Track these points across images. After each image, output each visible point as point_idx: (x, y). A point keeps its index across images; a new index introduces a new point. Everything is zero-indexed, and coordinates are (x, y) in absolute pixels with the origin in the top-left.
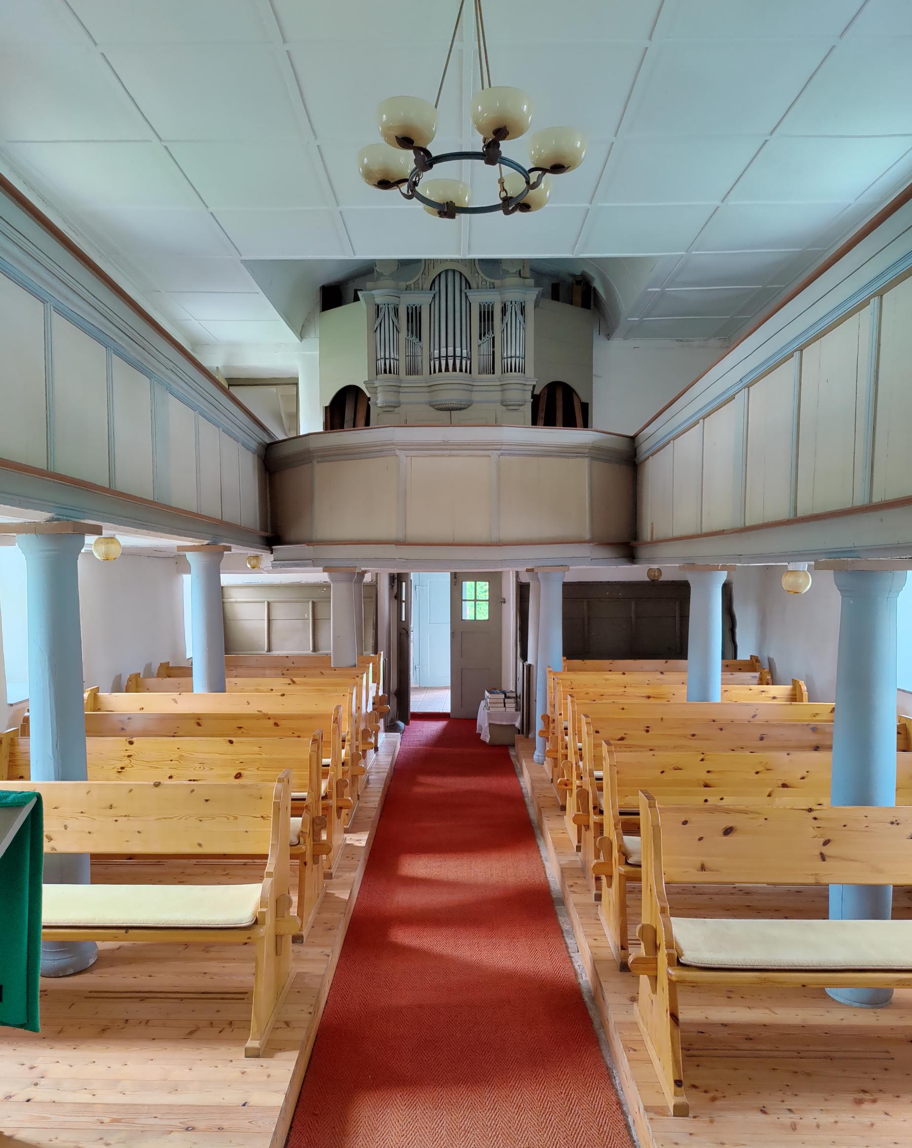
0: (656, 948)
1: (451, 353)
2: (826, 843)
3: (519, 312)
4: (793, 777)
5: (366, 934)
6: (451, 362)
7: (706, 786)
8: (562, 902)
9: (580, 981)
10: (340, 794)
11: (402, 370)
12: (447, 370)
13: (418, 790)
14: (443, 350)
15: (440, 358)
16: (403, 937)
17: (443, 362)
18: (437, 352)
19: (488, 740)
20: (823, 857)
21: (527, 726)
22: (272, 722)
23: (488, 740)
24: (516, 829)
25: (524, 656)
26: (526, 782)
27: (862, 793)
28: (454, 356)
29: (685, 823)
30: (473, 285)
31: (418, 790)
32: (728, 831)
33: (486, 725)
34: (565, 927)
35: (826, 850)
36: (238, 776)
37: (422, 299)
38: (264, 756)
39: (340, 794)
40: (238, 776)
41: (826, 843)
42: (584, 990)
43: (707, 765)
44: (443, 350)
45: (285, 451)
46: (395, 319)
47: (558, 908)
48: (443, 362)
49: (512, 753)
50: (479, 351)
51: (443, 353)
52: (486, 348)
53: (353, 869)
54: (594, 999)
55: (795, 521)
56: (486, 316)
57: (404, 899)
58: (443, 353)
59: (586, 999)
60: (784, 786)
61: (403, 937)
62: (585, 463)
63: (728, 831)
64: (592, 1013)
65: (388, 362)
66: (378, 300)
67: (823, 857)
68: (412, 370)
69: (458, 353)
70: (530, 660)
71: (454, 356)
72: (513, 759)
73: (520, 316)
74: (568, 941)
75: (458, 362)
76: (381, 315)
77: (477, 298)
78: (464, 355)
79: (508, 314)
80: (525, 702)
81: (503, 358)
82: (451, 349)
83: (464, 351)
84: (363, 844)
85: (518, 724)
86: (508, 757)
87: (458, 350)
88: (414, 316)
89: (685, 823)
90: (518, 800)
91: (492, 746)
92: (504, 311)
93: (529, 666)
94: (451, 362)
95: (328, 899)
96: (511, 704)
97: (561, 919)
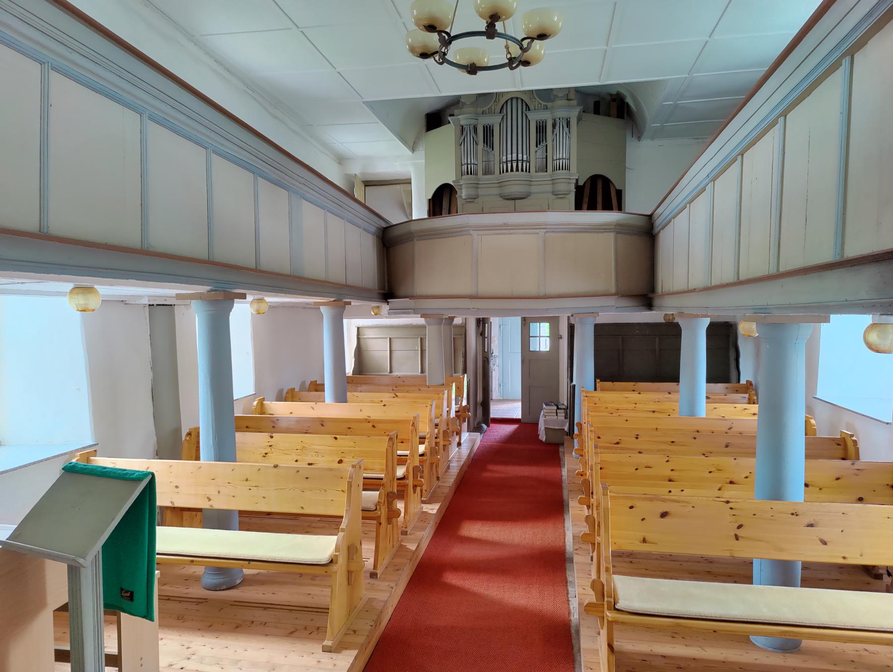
1: (514, 158)
2: (740, 527)
3: (565, 126)
4: (738, 476)
5: (426, 575)
6: (515, 165)
7: (670, 480)
8: (571, 561)
9: (572, 618)
11: (480, 172)
12: (512, 170)
13: (486, 475)
15: (507, 162)
16: (452, 578)
17: (509, 165)
18: (504, 157)
19: (544, 440)
20: (737, 537)
22: (371, 424)
23: (544, 440)
24: (552, 506)
25: (572, 381)
26: (564, 472)
27: (776, 491)
28: (517, 160)
29: (631, 507)
30: (532, 107)
31: (486, 475)
32: (664, 515)
33: (543, 428)
34: (570, 579)
35: (740, 532)
36: (340, 462)
37: (494, 120)
38: (357, 449)
39: (415, 477)
40: (340, 462)
41: (740, 527)
43: (671, 465)
45: (395, 232)
47: (568, 565)
49: (561, 449)
50: (536, 155)
51: (509, 159)
52: (540, 153)
53: (424, 529)
54: (578, 632)
55: (739, 283)
56: (541, 129)
57: (459, 552)
58: (509, 159)
59: (573, 631)
60: (731, 482)
61: (452, 578)
62: (612, 236)
63: (664, 515)
66: (462, 123)
67: (737, 537)
68: (487, 172)
69: (520, 158)
70: (574, 383)
71: (517, 160)
72: (561, 454)
73: (566, 129)
74: (570, 589)
75: (520, 164)
76: (465, 133)
77: (534, 117)
78: (525, 159)
79: (557, 127)
82: (514, 155)
83: (525, 156)
84: (435, 512)
85: (566, 429)
86: (558, 451)
87: (520, 156)
88: (488, 132)
89: (631, 507)
90: (557, 485)
91: (547, 444)
92: (554, 126)
93: (574, 386)
94: (515, 165)
96: (561, 414)
97: (568, 573)
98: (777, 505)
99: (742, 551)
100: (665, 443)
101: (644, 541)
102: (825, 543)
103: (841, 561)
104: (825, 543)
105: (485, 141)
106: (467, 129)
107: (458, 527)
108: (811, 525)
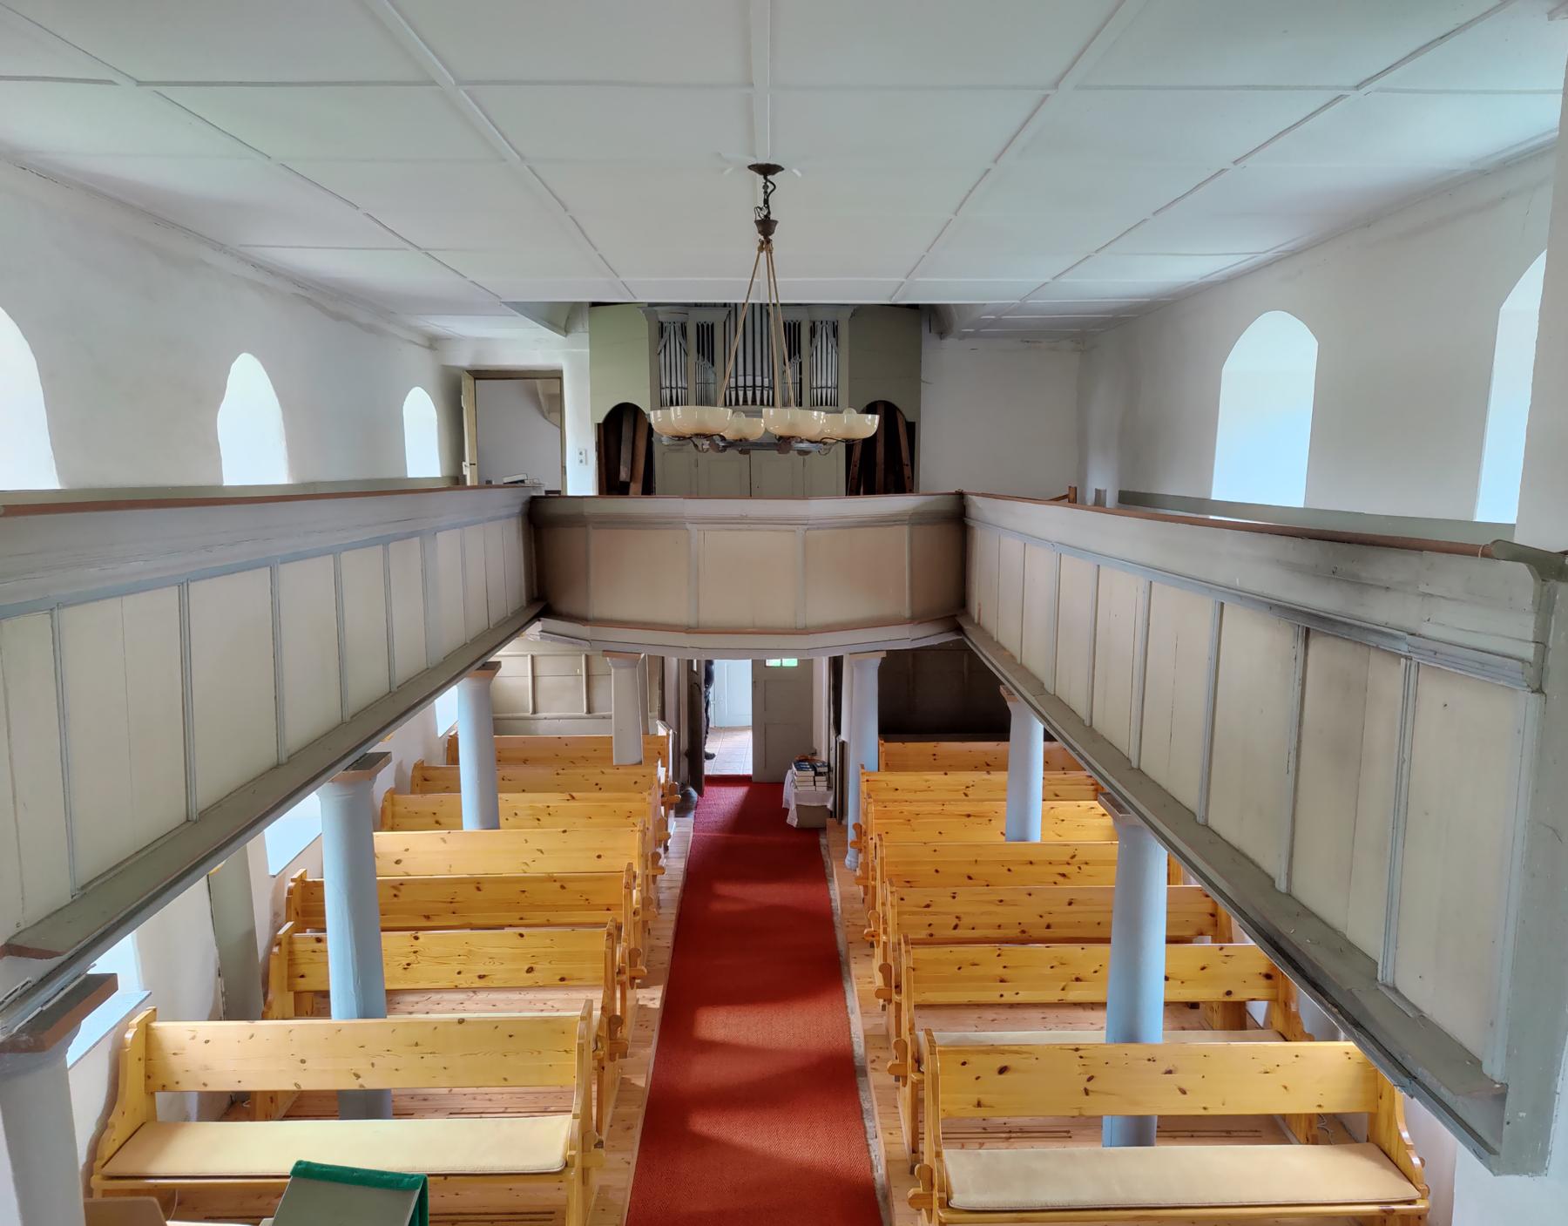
0: (932, 1185)
1: (749, 382)
2: (1090, 1079)
5: (666, 1122)
6: (750, 394)
8: (865, 1073)
9: (876, 1175)
10: (633, 964)
12: (745, 402)
13: (717, 906)
14: (741, 379)
16: (703, 1124)
17: (741, 394)
19: (795, 824)
20: (1087, 1092)
21: (840, 811)
23: (795, 824)
25: (838, 731)
26: (836, 890)
28: (754, 386)
31: (717, 906)
32: (1003, 1070)
33: (793, 807)
34: (866, 1106)
35: (1089, 1086)
39: (633, 964)
41: (1090, 1079)
42: (878, 1186)
43: (1004, 961)
44: (741, 379)
45: (557, 508)
47: (860, 1079)
48: (741, 394)
49: (823, 841)
51: (741, 383)
53: (648, 1044)
54: (886, 1197)
57: (705, 1072)
58: (741, 383)
59: (879, 1198)
60: (1077, 979)
61: (703, 1124)
62: (905, 530)
63: (1003, 1070)
64: (883, 1214)
67: (1087, 1092)
69: (758, 383)
70: (843, 737)
71: (754, 386)
72: (824, 852)
74: (868, 1124)
76: (666, 335)
79: (818, 336)
80: (837, 776)
84: (657, 1004)
85: (829, 806)
86: (817, 846)
87: (758, 379)
91: (800, 830)
93: (843, 744)
94: (750, 394)
95: (625, 1083)
96: (822, 782)
97: (862, 1094)
98: (1131, 1048)
99: (1092, 1106)
100: (991, 902)
101: (979, 1105)
102: (1184, 1092)
103: (1202, 1112)
104: (1184, 1092)
105: (701, 350)
106: (670, 329)
107: (690, 1024)
108: (1170, 1072)
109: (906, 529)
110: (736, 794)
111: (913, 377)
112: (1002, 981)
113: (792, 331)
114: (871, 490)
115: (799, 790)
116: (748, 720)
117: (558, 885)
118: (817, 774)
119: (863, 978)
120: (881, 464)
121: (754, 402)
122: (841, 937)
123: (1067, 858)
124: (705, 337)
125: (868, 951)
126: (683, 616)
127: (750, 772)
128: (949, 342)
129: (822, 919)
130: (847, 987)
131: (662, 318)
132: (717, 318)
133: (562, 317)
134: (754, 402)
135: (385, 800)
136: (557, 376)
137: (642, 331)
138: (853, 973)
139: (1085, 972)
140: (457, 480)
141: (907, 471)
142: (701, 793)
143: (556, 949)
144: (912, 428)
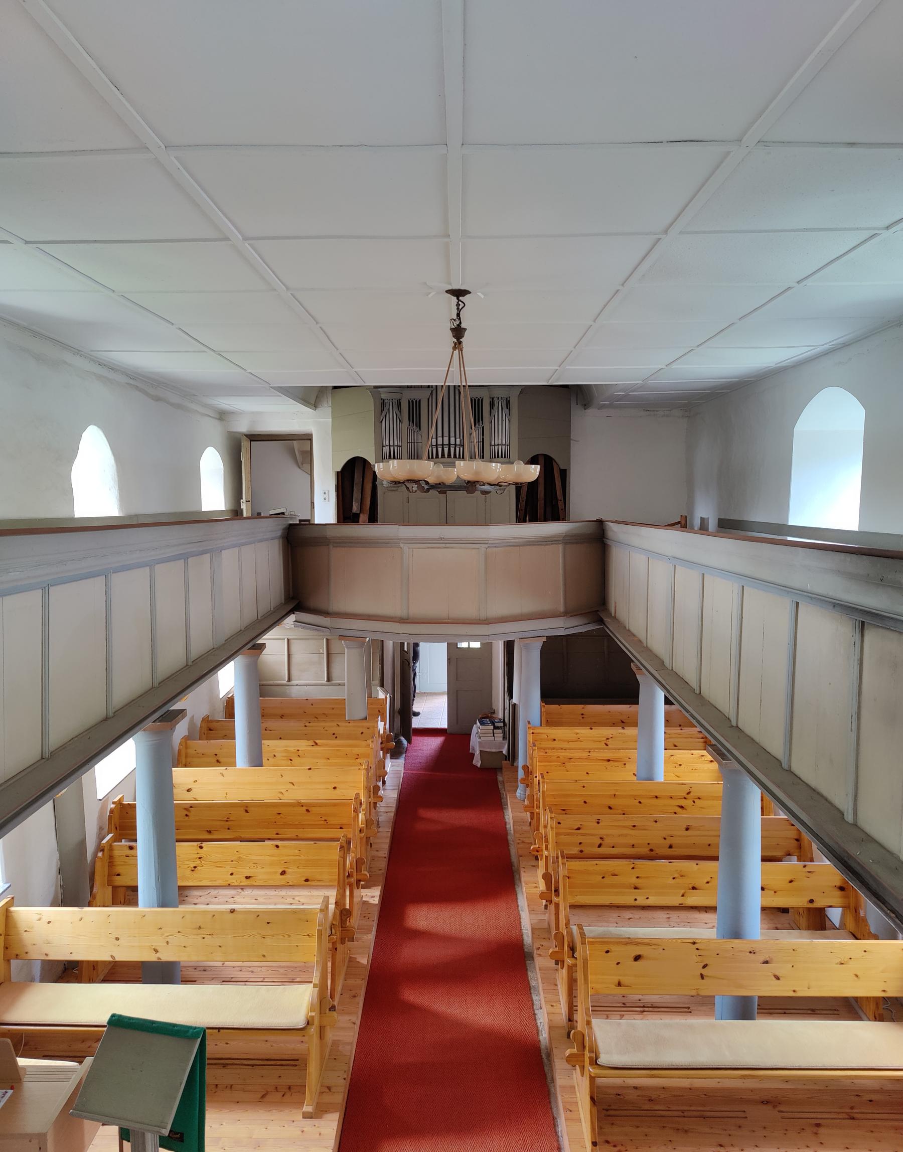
1: (446, 441)
6: (446, 450)
14: (440, 439)
17: (440, 450)
25: (511, 697)
28: (449, 445)
44: (440, 439)
46: (398, 414)
48: (440, 450)
51: (440, 442)
58: (440, 442)
65: (392, 448)
69: (453, 442)
70: (515, 700)
71: (449, 445)
72: (500, 786)
78: (458, 443)
81: (491, 445)
83: (458, 440)
87: (452, 439)
94: (446, 450)
109: (560, 547)
110: (435, 743)
111: (565, 438)
112: (636, 888)
113: (477, 405)
114: (534, 519)
115: (482, 739)
116: (445, 688)
117: (304, 809)
118: (496, 728)
119: (531, 884)
120: (542, 500)
121: (449, 456)
122: (513, 851)
123: (684, 794)
124: (415, 409)
125: (534, 863)
126: (397, 610)
127: (446, 726)
128: (591, 411)
129: (500, 838)
130: (518, 890)
131: (383, 396)
132: (423, 396)
133: (312, 397)
134: (449, 456)
135: (181, 744)
136: (308, 438)
137: (369, 406)
138: (523, 879)
139: (700, 882)
140: (236, 513)
141: (561, 504)
142: (409, 742)
143: (303, 857)
144: (564, 474)
